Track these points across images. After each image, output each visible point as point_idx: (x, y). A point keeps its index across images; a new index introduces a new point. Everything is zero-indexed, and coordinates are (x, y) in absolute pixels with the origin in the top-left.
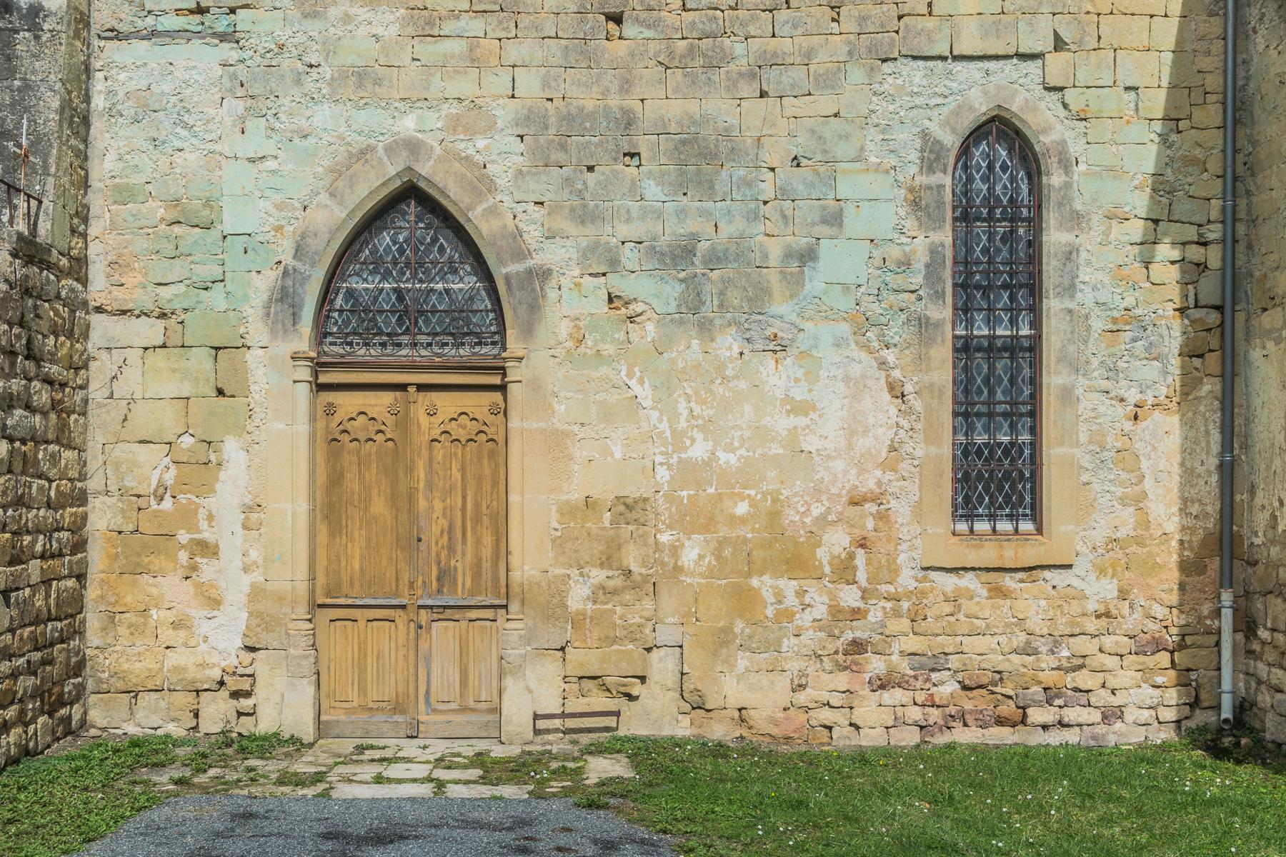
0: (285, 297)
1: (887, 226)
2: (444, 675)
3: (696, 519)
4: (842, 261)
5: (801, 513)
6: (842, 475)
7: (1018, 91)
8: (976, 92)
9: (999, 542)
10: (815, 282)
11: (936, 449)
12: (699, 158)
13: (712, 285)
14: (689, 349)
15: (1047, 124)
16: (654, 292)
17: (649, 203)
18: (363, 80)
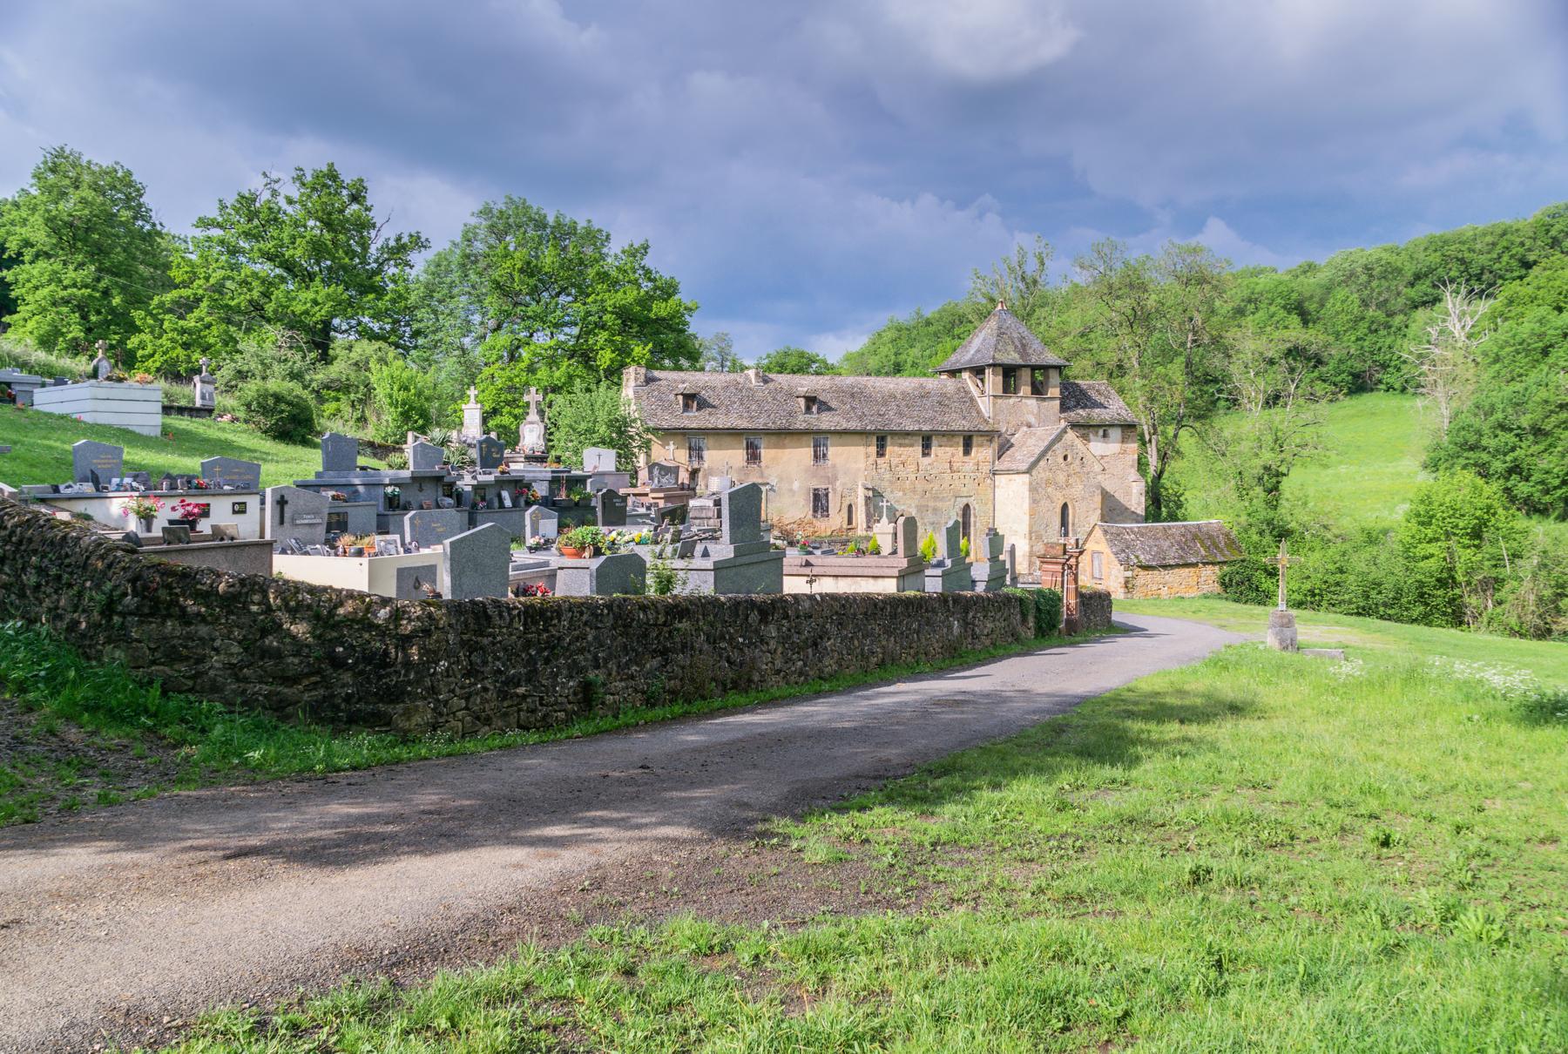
8: (965, 501)
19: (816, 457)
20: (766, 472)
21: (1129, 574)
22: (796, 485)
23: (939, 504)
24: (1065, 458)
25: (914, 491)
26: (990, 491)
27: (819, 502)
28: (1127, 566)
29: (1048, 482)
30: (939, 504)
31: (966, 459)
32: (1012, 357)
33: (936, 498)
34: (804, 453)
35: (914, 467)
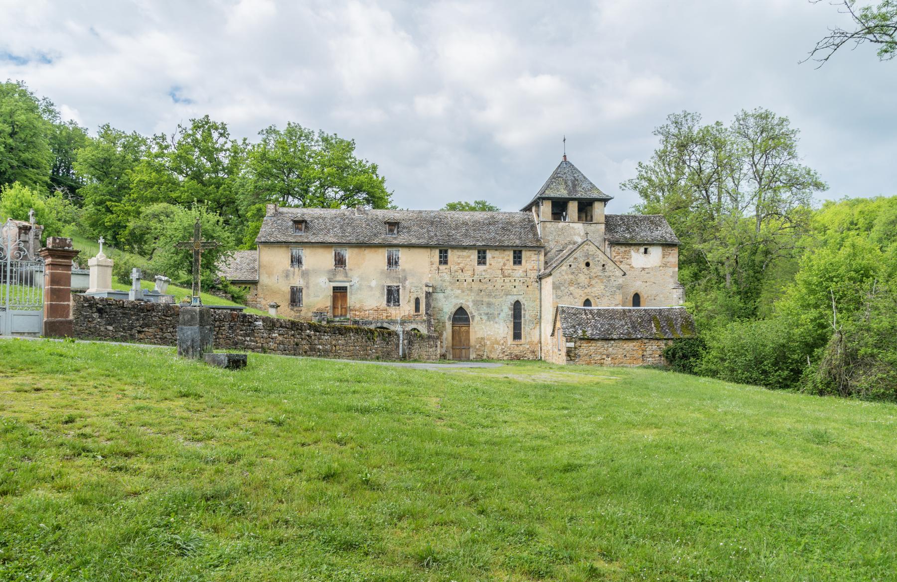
0: (449, 318)
1: (507, 312)
2: (464, 355)
3: (488, 339)
4: (503, 315)
5: (499, 338)
6: (503, 335)
9: (517, 342)
10: (501, 316)
11: (511, 333)
12: (489, 305)
13: (490, 317)
14: (488, 323)
15: (523, 301)
16: (485, 318)
17: (484, 309)
18: (457, 297)
20: (350, 274)
21: (572, 345)
22: (373, 284)
23: (492, 300)
24: (588, 264)
25: (471, 289)
26: (537, 292)
27: (392, 296)
28: (569, 339)
29: (571, 283)
30: (492, 300)
31: (517, 267)
32: (563, 193)
33: (489, 295)
34: (377, 259)
35: (470, 273)
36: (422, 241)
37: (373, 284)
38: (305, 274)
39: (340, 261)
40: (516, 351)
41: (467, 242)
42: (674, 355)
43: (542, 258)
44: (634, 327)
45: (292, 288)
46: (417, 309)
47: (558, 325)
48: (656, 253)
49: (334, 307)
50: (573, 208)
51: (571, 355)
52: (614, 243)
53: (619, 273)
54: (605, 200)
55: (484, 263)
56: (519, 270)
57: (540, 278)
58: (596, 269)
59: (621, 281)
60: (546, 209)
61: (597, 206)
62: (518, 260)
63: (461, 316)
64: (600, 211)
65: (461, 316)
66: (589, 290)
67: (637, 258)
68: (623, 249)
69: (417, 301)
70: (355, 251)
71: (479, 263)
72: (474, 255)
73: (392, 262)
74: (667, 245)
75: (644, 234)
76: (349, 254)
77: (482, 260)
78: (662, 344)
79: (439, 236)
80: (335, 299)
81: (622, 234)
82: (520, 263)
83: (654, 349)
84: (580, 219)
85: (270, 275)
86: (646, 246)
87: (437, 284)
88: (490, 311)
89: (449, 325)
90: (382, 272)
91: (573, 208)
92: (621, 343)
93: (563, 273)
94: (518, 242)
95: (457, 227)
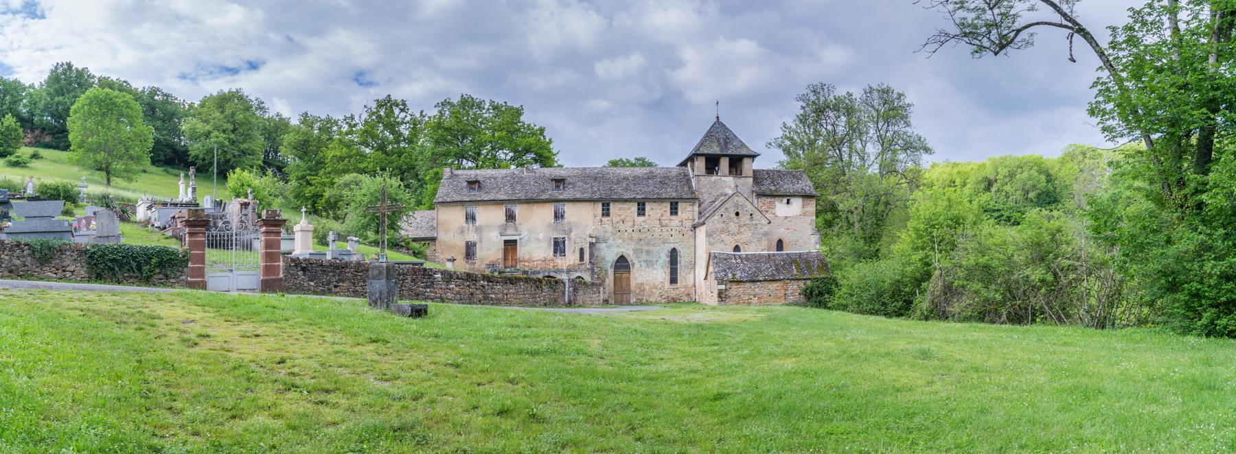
1: (665, 258)
4: (661, 261)
7: (676, 246)
8: (672, 246)
9: (674, 286)
11: (668, 278)
12: (648, 252)
13: (649, 264)
16: (644, 265)
17: (644, 257)
19: (556, 217)
21: (723, 287)
22: (541, 236)
23: (651, 248)
24: (737, 214)
25: (631, 239)
27: (559, 247)
28: (721, 282)
29: (722, 231)
30: (651, 248)
31: (673, 217)
33: (648, 244)
35: (631, 223)
36: (586, 196)
37: (541, 236)
38: (478, 230)
39: (511, 217)
40: (673, 294)
41: (627, 196)
42: (811, 293)
43: (696, 208)
44: (777, 270)
45: (467, 243)
46: (582, 258)
47: (711, 269)
48: (797, 203)
49: (505, 259)
50: (724, 164)
51: (722, 296)
52: (760, 195)
53: (764, 222)
54: (753, 157)
55: (644, 215)
56: (676, 220)
57: (695, 227)
58: (744, 218)
59: (766, 228)
60: (700, 164)
61: (746, 161)
62: (674, 210)
63: (622, 264)
64: (749, 166)
65: (622, 264)
66: (738, 237)
67: (781, 209)
68: (769, 200)
69: (582, 250)
70: (525, 206)
71: (639, 215)
72: (634, 208)
73: (558, 216)
74: (806, 196)
75: (787, 186)
76: (518, 210)
77: (641, 212)
78: (801, 284)
79: (600, 190)
80: (506, 251)
81: (767, 186)
82: (676, 213)
83: (795, 288)
84: (730, 173)
85: (447, 232)
86: (788, 197)
87: (601, 235)
88: (649, 258)
89: (611, 272)
90: (549, 225)
91: (724, 164)
92: (766, 284)
93: (715, 222)
94: (674, 194)
95: (618, 182)
